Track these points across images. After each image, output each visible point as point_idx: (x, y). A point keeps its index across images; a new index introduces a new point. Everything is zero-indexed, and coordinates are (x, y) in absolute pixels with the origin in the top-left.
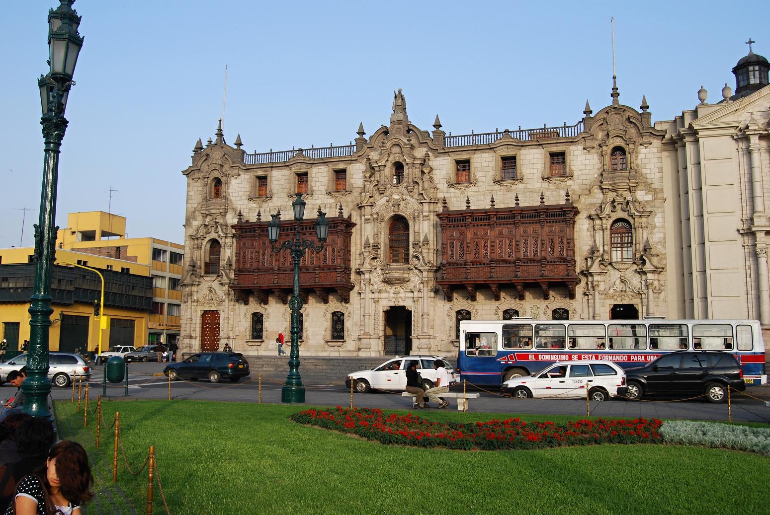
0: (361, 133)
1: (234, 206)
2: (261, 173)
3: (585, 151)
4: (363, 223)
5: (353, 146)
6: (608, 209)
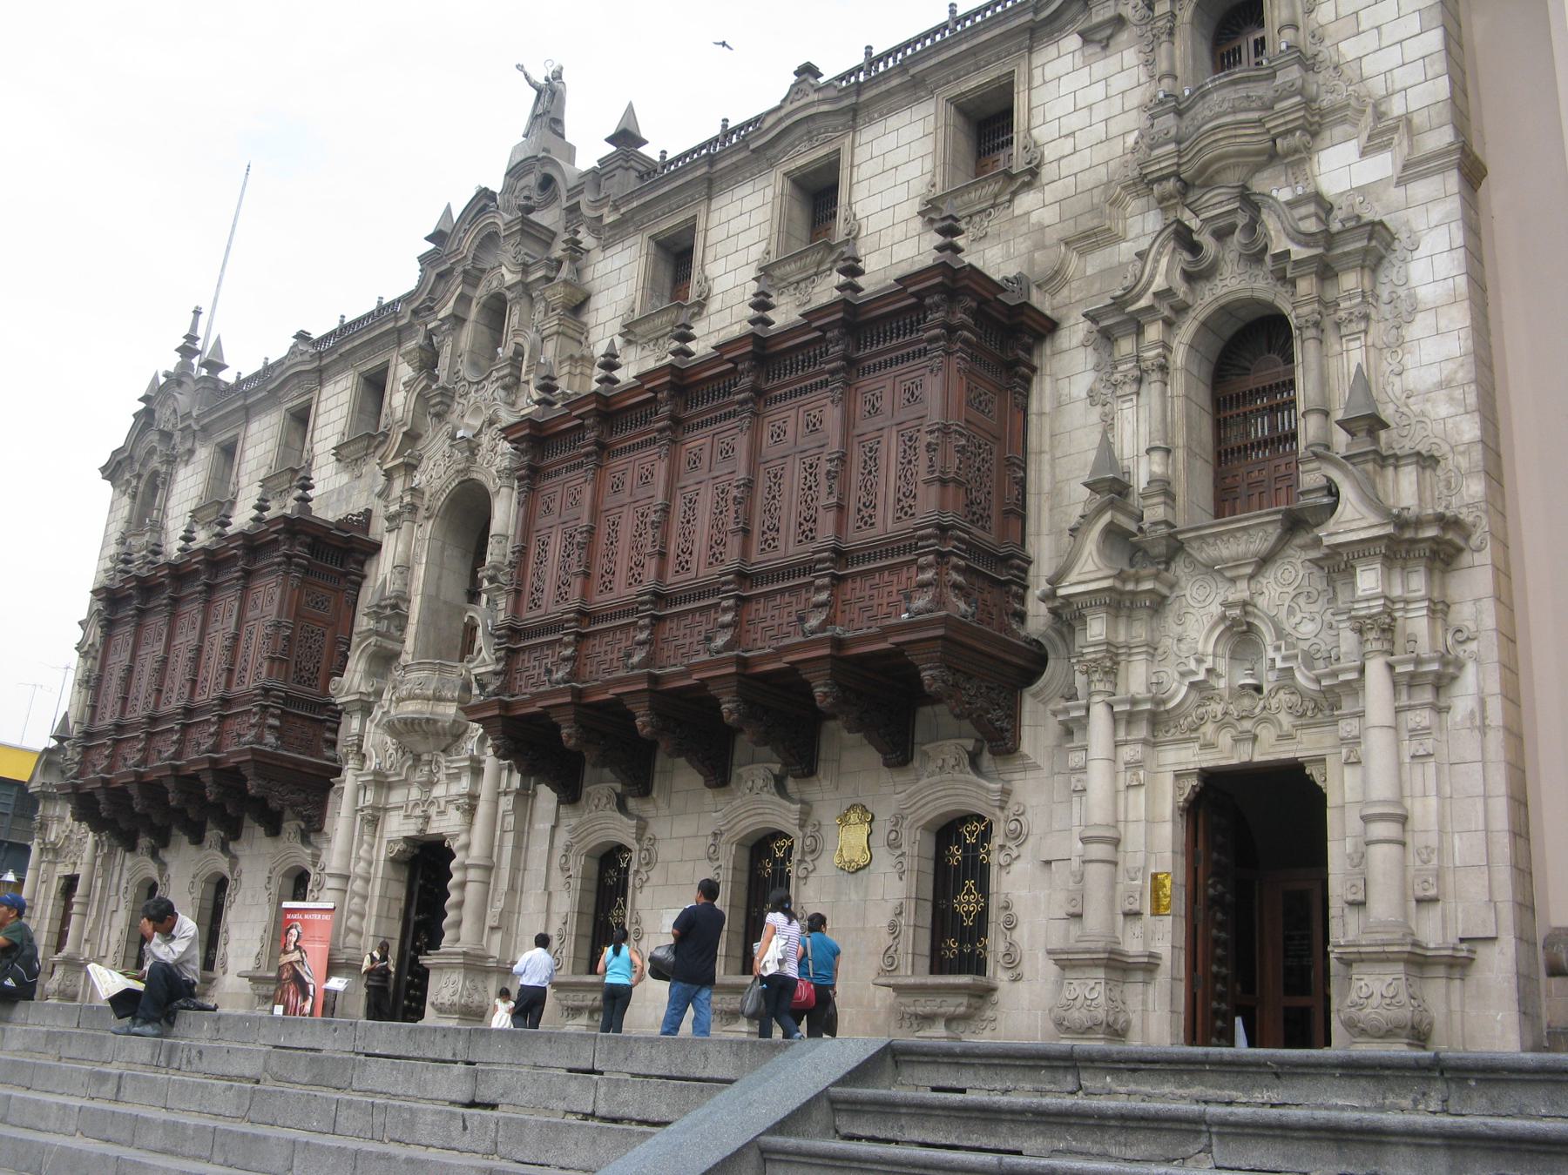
3: (1091, 50)
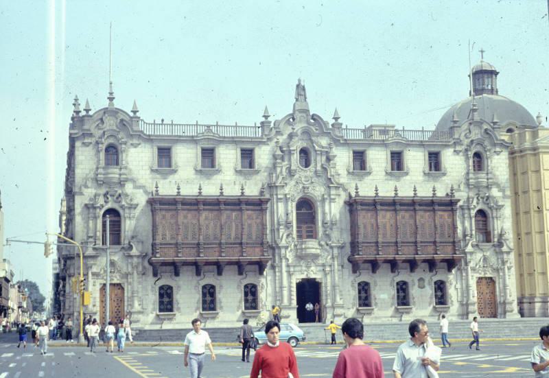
1: (134, 176)
4: (275, 200)
6: (475, 201)
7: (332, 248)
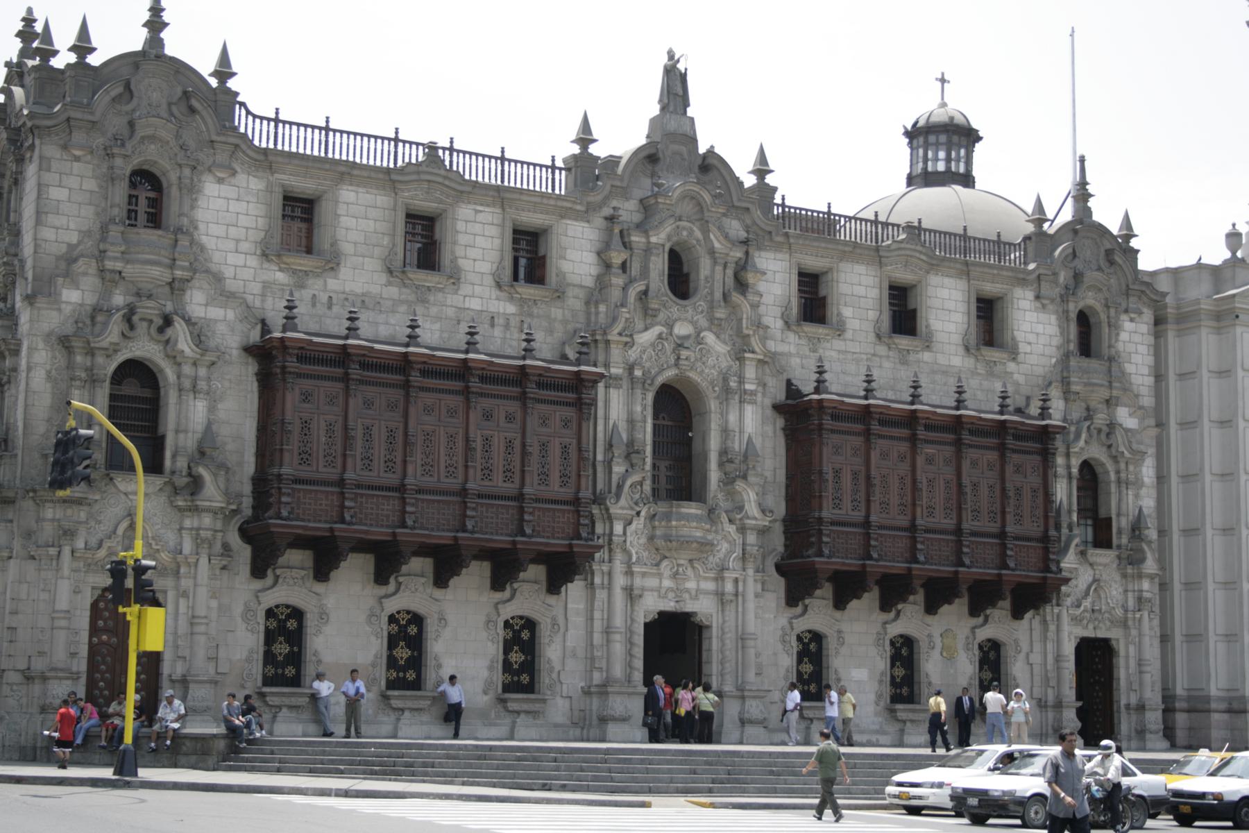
0: (585, 138)
1: (214, 268)
2: (304, 185)
3: (1038, 305)
5: (560, 169)
7: (742, 530)
